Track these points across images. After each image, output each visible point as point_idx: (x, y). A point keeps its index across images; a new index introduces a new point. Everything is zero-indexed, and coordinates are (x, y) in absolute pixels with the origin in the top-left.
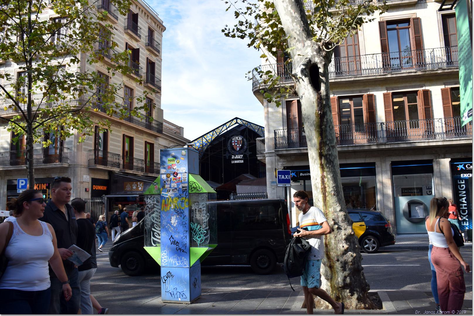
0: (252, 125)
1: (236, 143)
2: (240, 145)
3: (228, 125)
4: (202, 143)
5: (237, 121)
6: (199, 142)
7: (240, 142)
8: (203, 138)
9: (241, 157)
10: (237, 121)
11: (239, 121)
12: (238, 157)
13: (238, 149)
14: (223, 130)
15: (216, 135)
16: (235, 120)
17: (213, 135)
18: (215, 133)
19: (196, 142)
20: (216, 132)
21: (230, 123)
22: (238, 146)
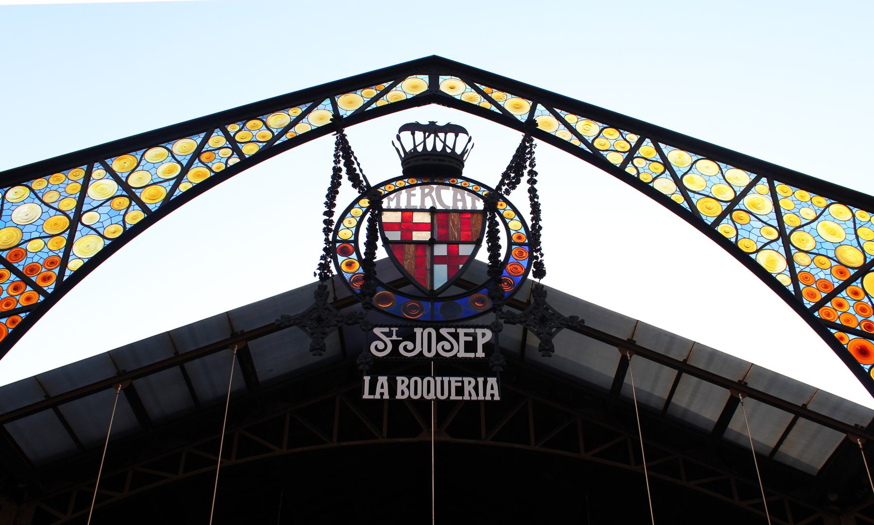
1: (421, 227)
3: (349, 103)
4: (69, 205)
5: (434, 83)
8: (98, 172)
9: (471, 346)
10: (434, 83)
11: (450, 85)
12: (438, 348)
14: (301, 128)
15: (220, 161)
16: (418, 84)
17: (197, 154)
18: (223, 141)
20: (231, 139)
21: (372, 92)
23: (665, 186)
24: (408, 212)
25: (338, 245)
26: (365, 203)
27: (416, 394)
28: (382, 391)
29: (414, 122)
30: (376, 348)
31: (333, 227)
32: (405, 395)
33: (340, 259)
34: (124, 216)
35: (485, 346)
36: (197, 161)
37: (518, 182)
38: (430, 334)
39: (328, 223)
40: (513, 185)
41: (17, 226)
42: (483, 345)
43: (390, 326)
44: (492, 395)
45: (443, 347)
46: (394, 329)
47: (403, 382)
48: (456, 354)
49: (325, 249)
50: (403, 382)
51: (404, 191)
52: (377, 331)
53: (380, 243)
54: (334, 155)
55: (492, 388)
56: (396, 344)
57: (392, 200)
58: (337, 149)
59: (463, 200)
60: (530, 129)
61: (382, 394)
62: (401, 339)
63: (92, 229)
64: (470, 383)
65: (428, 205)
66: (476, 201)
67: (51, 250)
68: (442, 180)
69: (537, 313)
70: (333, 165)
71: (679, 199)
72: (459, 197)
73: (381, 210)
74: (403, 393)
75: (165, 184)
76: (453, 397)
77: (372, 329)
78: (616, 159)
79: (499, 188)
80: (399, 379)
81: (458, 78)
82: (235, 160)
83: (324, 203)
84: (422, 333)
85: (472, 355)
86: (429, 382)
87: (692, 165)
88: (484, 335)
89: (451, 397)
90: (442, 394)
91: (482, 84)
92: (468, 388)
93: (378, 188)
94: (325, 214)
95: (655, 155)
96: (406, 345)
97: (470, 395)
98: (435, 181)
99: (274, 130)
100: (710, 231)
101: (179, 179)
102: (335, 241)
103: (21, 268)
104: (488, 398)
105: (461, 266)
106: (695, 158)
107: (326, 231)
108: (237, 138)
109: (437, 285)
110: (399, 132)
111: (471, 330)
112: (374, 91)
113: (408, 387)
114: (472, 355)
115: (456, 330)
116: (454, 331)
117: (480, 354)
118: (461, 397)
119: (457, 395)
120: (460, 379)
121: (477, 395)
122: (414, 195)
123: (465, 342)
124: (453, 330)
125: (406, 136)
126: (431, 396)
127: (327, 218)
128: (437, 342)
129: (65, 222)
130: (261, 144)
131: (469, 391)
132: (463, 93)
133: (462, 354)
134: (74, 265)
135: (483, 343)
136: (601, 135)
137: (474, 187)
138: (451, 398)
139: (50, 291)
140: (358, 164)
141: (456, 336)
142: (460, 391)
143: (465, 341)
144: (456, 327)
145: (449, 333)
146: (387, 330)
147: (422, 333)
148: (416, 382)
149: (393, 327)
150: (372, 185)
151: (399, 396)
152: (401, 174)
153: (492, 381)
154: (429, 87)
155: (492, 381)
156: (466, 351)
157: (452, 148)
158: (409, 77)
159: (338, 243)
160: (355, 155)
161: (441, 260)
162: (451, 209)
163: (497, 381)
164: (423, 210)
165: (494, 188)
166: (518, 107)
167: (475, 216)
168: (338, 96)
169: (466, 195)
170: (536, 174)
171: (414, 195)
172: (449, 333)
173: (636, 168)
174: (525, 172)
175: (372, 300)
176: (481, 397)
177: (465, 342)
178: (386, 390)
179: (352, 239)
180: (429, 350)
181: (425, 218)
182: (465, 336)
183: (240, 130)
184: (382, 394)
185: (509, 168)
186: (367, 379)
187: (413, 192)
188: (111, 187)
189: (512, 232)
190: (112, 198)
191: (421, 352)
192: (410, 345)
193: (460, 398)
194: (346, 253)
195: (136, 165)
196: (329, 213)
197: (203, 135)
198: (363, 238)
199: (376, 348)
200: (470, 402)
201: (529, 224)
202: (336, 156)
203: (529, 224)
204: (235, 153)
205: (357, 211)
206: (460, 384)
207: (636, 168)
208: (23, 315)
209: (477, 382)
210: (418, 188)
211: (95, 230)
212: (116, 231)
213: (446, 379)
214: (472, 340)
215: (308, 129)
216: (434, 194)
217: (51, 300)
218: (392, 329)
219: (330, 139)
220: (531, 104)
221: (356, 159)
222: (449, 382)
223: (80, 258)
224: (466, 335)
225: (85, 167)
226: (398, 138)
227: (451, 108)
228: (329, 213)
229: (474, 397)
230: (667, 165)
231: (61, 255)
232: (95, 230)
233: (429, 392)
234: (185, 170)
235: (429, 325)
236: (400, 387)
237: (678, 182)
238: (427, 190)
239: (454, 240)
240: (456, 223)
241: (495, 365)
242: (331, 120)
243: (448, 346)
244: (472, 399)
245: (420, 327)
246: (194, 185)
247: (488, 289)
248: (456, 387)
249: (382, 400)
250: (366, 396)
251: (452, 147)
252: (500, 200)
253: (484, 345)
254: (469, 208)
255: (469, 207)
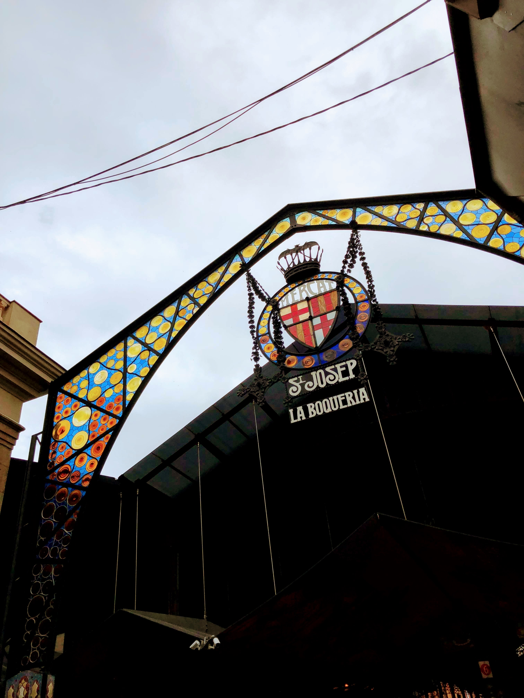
0: (378, 209)
1: (303, 311)
2: (331, 316)
4: (120, 365)
6: (110, 365)
7: (328, 302)
9: (345, 373)
12: (326, 380)
13: (320, 337)
14: (226, 279)
19: (94, 368)
20: (192, 298)
21: (261, 240)
22: (317, 321)
23: (449, 229)
24: (294, 305)
25: (260, 338)
26: (270, 308)
27: (320, 411)
28: (301, 415)
29: (286, 250)
30: (292, 390)
31: (255, 329)
32: (314, 415)
33: (263, 345)
34: (148, 361)
35: (354, 371)
36: (178, 316)
37: (354, 262)
38: (320, 373)
39: (252, 327)
40: (351, 266)
41: (98, 385)
42: (352, 370)
43: (297, 376)
44: (364, 399)
45: (329, 379)
46: (300, 377)
47: (311, 406)
48: (338, 381)
49: (254, 343)
50: (311, 406)
51: (289, 294)
52: (291, 381)
53: (283, 329)
54: (247, 286)
55: (363, 395)
56: (303, 385)
57: (284, 301)
58: (248, 283)
59: (324, 286)
60: (354, 226)
61: (301, 417)
62: (305, 381)
63: (134, 374)
64: (349, 395)
65: (304, 296)
66: (331, 284)
67: (117, 393)
68: (309, 278)
69: (382, 339)
70: (248, 292)
71: (459, 234)
72: (321, 285)
73: (279, 310)
74: (313, 413)
75: (165, 335)
76: (342, 407)
77: (288, 381)
78: (412, 224)
79: (342, 271)
80: (309, 405)
81: (307, 212)
82: (197, 309)
83: (248, 317)
84: (316, 374)
85: (347, 378)
86: (326, 402)
87: (464, 207)
88: (351, 364)
89: (340, 407)
90: (335, 407)
91: (320, 210)
92: (349, 399)
93: (275, 297)
94: (250, 322)
95: (437, 211)
96: (308, 384)
97: (351, 403)
98: (306, 281)
99: (213, 284)
100: (485, 247)
101: (171, 330)
102: (258, 336)
103: (104, 408)
104: (362, 401)
105: (330, 327)
106: (465, 202)
107: (252, 332)
108: (195, 297)
109: (319, 342)
110: (279, 260)
111: (344, 363)
112: (261, 239)
113: (315, 409)
114: (347, 378)
115: (335, 366)
116: (345, 364)
117: (352, 376)
118: (346, 405)
119: (343, 405)
120: (343, 395)
121: (355, 401)
122: (296, 294)
123: (342, 372)
124: (333, 367)
125: (283, 260)
126: (329, 410)
127: (251, 324)
128: (326, 377)
129: (120, 375)
130: (208, 295)
131: (350, 401)
132: (311, 220)
133: (342, 379)
134: (129, 397)
135: (352, 369)
136: (400, 212)
137: (328, 275)
138: (341, 408)
139: (120, 416)
140: (261, 287)
141: (335, 370)
142: (345, 402)
143: (341, 371)
144: (334, 364)
145: (332, 369)
146: (296, 379)
147: (316, 374)
148: (318, 404)
149: (299, 376)
150: (271, 297)
151: (311, 416)
152: (287, 284)
153: (362, 390)
154: (291, 224)
155: (362, 390)
156: (343, 376)
157: (309, 256)
158: (279, 223)
159: (259, 337)
160: (258, 282)
161: (318, 327)
162: (318, 294)
163: (365, 390)
164: (302, 301)
165: (340, 272)
166: (344, 214)
167: (333, 293)
168: (242, 251)
169: (325, 283)
170: (364, 253)
171: (296, 294)
172: (332, 369)
173: (426, 224)
174: (357, 254)
175: (284, 365)
176: (358, 402)
177: (342, 372)
178: (303, 415)
179: (267, 332)
180: (322, 383)
181: (305, 305)
182: (341, 368)
183: (196, 291)
184: (301, 417)
185: (347, 257)
186: (291, 411)
187: (294, 292)
188: (138, 347)
189: (356, 296)
190: (140, 353)
191: (318, 385)
192: (311, 384)
193: (345, 406)
194: (264, 341)
195: (148, 330)
196: (252, 322)
197: (177, 302)
198: (272, 330)
199: (292, 390)
200: (353, 407)
201: (366, 286)
202: (249, 287)
203: (366, 286)
204: (196, 305)
205: (267, 315)
206: (344, 398)
207: (426, 224)
208: (111, 433)
209: (353, 394)
210: (297, 289)
211: (135, 374)
212: (145, 371)
213: (335, 397)
214: (345, 369)
215: (231, 276)
216: (306, 289)
217: (122, 420)
218: (299, 377)
219: (244, 277)
220: (352, 210)
221: (259, 284)
222: (337, 398)
223: (131, 392)
224: (341, 367)
225: (123, 342)
226: (279, 264)
227: (307, 232)
228: (252, 322)
229: (354, 403)
230: (446, 214)
231: (122, 394)
232: (135, 374)
233: (327, 408)
234: (173, 324)
235: (319, 368)
236: (310, 410)
237: (456, 222)
238: (302, 288)
239: (323, 312)
240: (322, 302)
241: (361, 380)
242: (240, 267)
243: (332, 377)
244: (353, 405)
245: (314, 371)
246: (179, 331)
247: (349, 335)
248: (342, 400)
249: (302, 422)
250: (293, 421)
251: (309, 256)
252: (346, 278)
253: (353, 370)
254: (328, 289)
255: (328, 289)
